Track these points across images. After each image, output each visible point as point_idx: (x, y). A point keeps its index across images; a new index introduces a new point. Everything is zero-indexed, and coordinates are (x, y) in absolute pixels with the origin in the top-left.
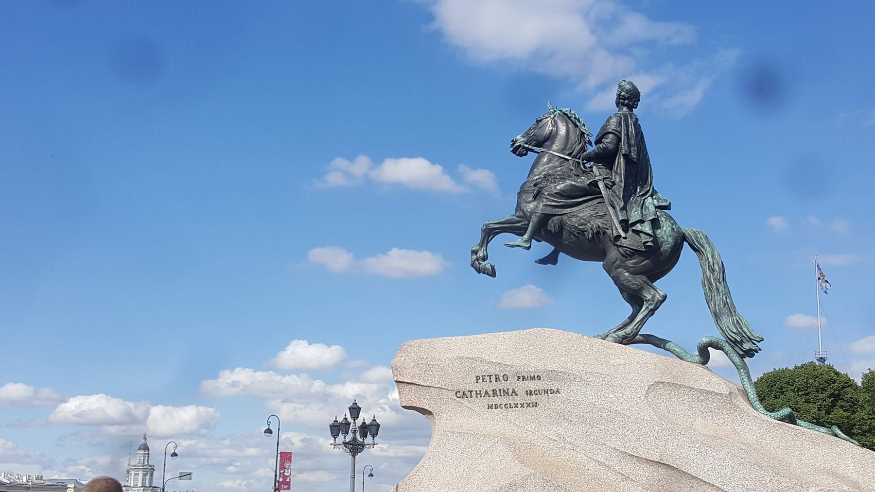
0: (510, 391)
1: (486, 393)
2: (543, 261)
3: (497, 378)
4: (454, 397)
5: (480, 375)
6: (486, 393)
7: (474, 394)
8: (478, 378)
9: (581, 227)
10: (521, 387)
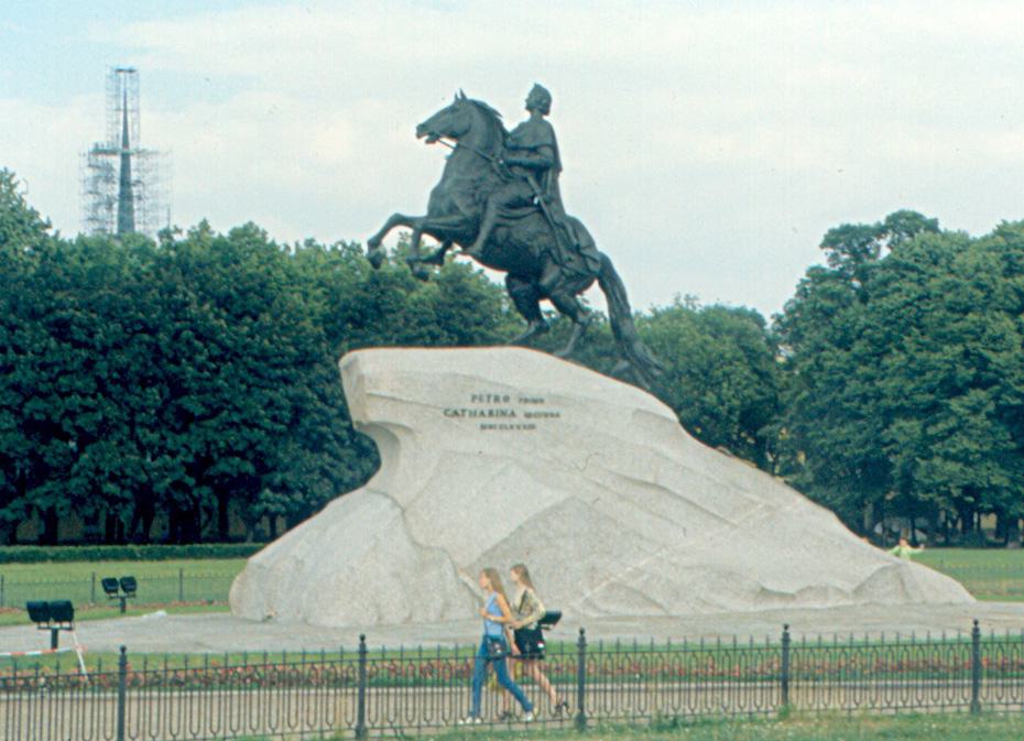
1: (482, 414)
3: (497, 399)
4: (443, 415)
7: (467, 414)
8: (474, 398)
10: (521, 409)
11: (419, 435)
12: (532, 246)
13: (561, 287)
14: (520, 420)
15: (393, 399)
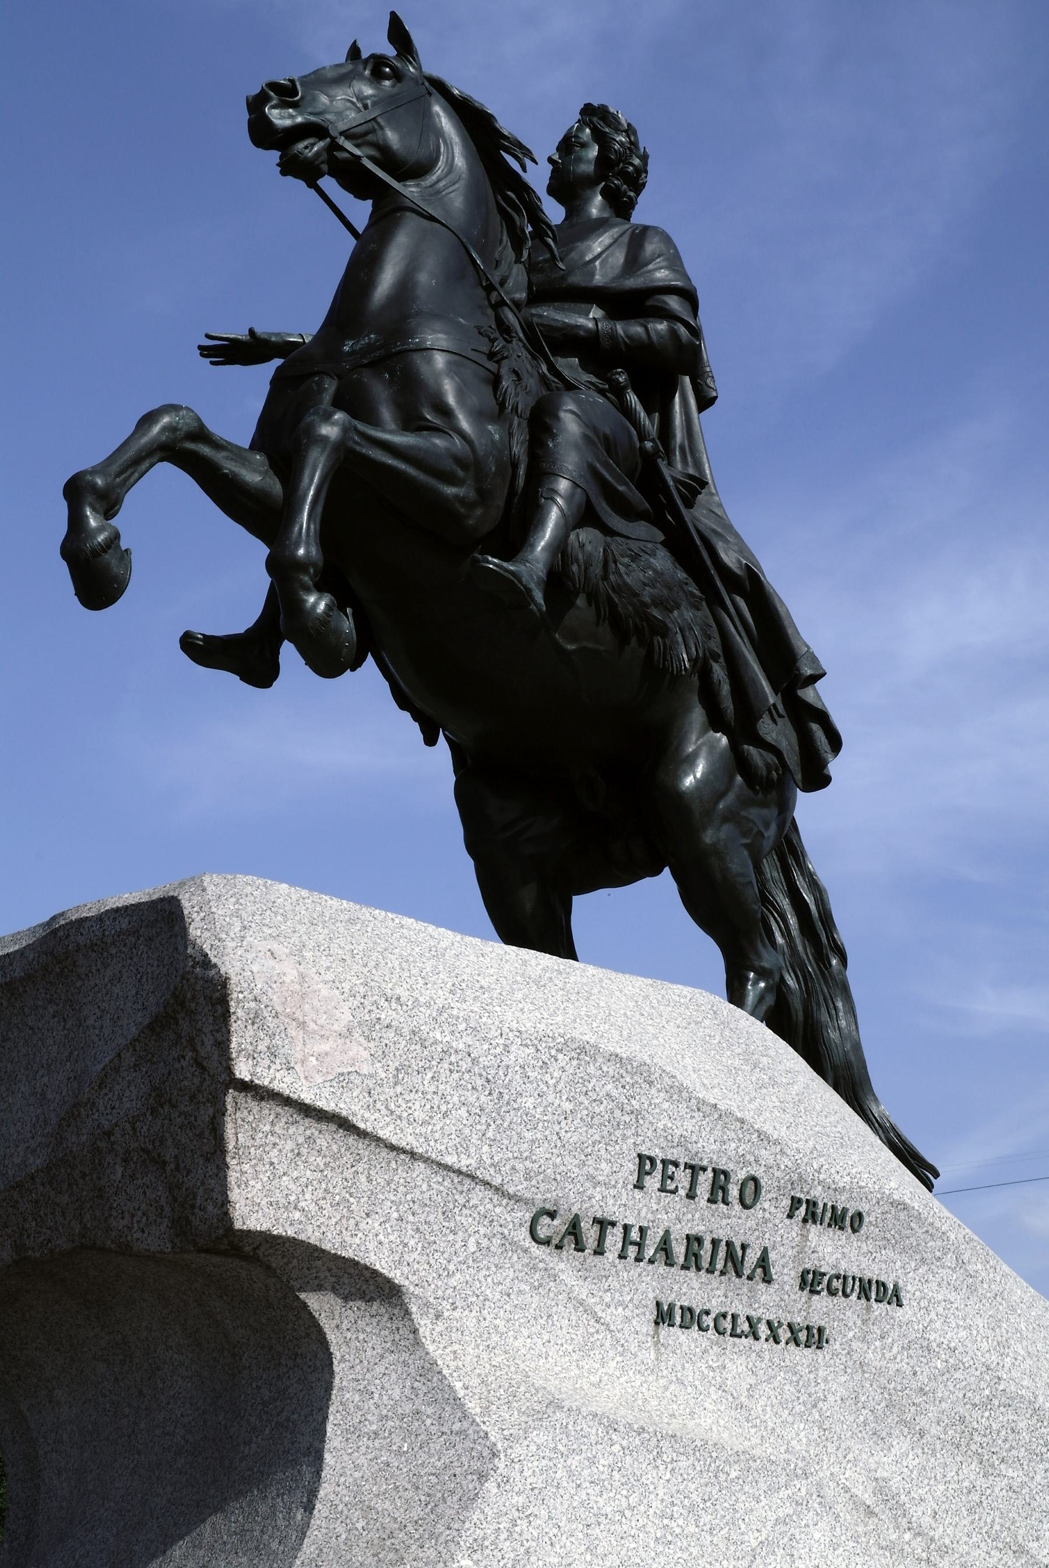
0: (752, 1257)
1: (665, 1246)
2: (203, 650)
4: (523, 1235)
5: (658, 1153)
6: (665, 1246)
7: (614, 1239)
9: (656, 613)
11: (424, 1325)
12: (663, 630)
13: (729, 817)
14: (778, 1300)
15: (344, 1124)
